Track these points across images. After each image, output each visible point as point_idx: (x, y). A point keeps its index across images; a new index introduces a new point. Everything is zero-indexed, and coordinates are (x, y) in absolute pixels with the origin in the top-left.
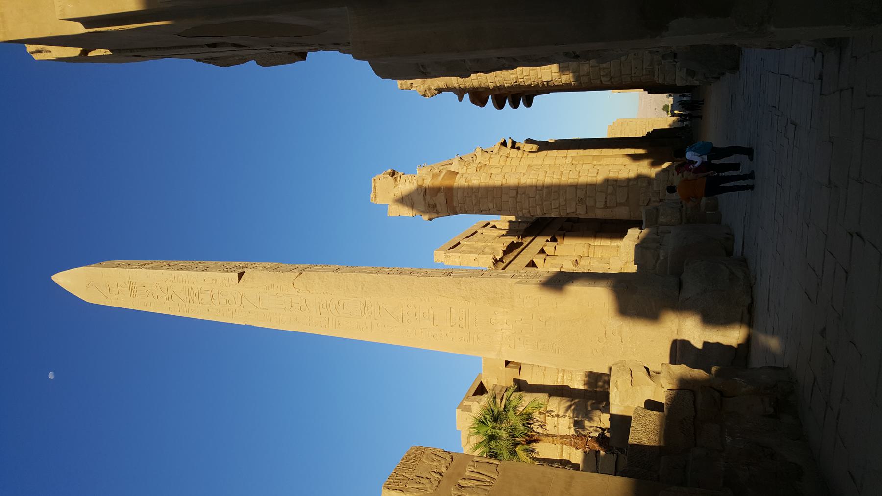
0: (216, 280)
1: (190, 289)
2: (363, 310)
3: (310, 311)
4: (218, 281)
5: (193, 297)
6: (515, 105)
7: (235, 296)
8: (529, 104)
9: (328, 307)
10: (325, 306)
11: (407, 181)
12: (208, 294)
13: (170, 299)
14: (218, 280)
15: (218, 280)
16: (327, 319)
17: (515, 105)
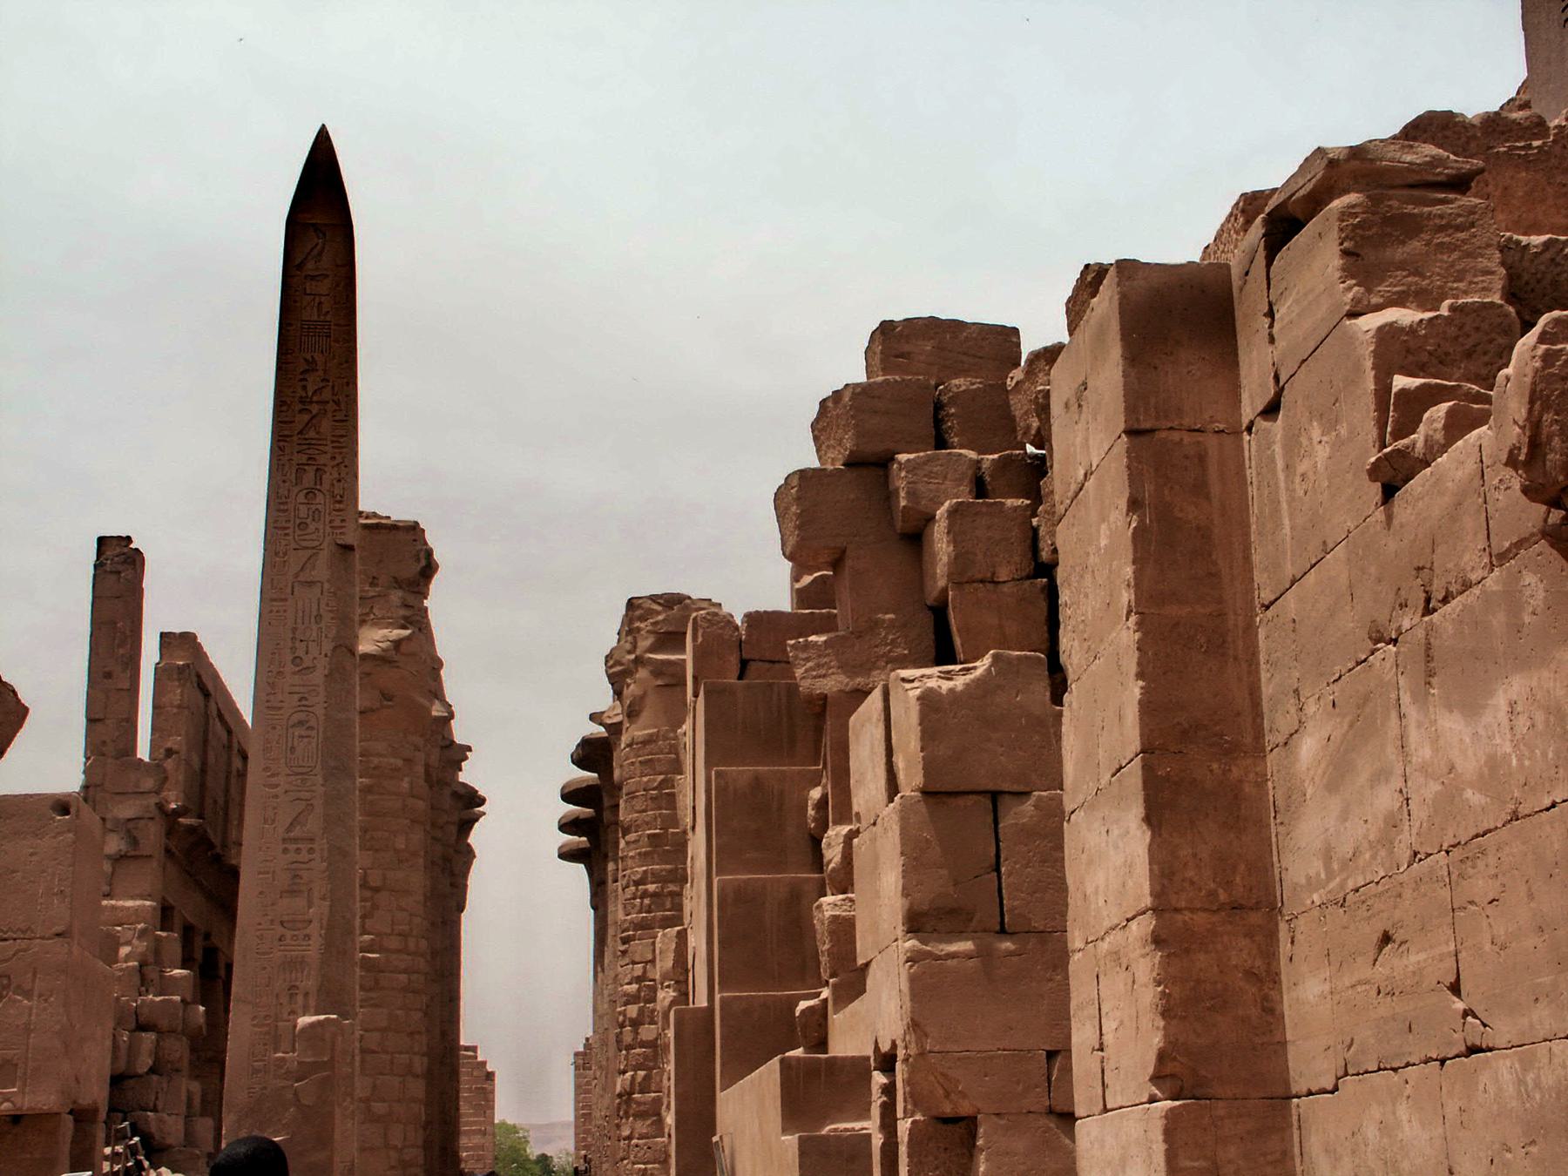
0: (340, 502)
1: (321, 448)
2: (300, 770)
3: (294, 673)
4: (337, 506)
5: (308, 451)
6: (567, 826)
7: (314, 536)
8: (567, 855)
9: (303, 708)
10: (304, 702)
11: (407, 613)
12: (316, 484)
13: (301, 406)
14: (342, 506)
15: (342, 506)
16: (280, 705)
17: (567, 826)
